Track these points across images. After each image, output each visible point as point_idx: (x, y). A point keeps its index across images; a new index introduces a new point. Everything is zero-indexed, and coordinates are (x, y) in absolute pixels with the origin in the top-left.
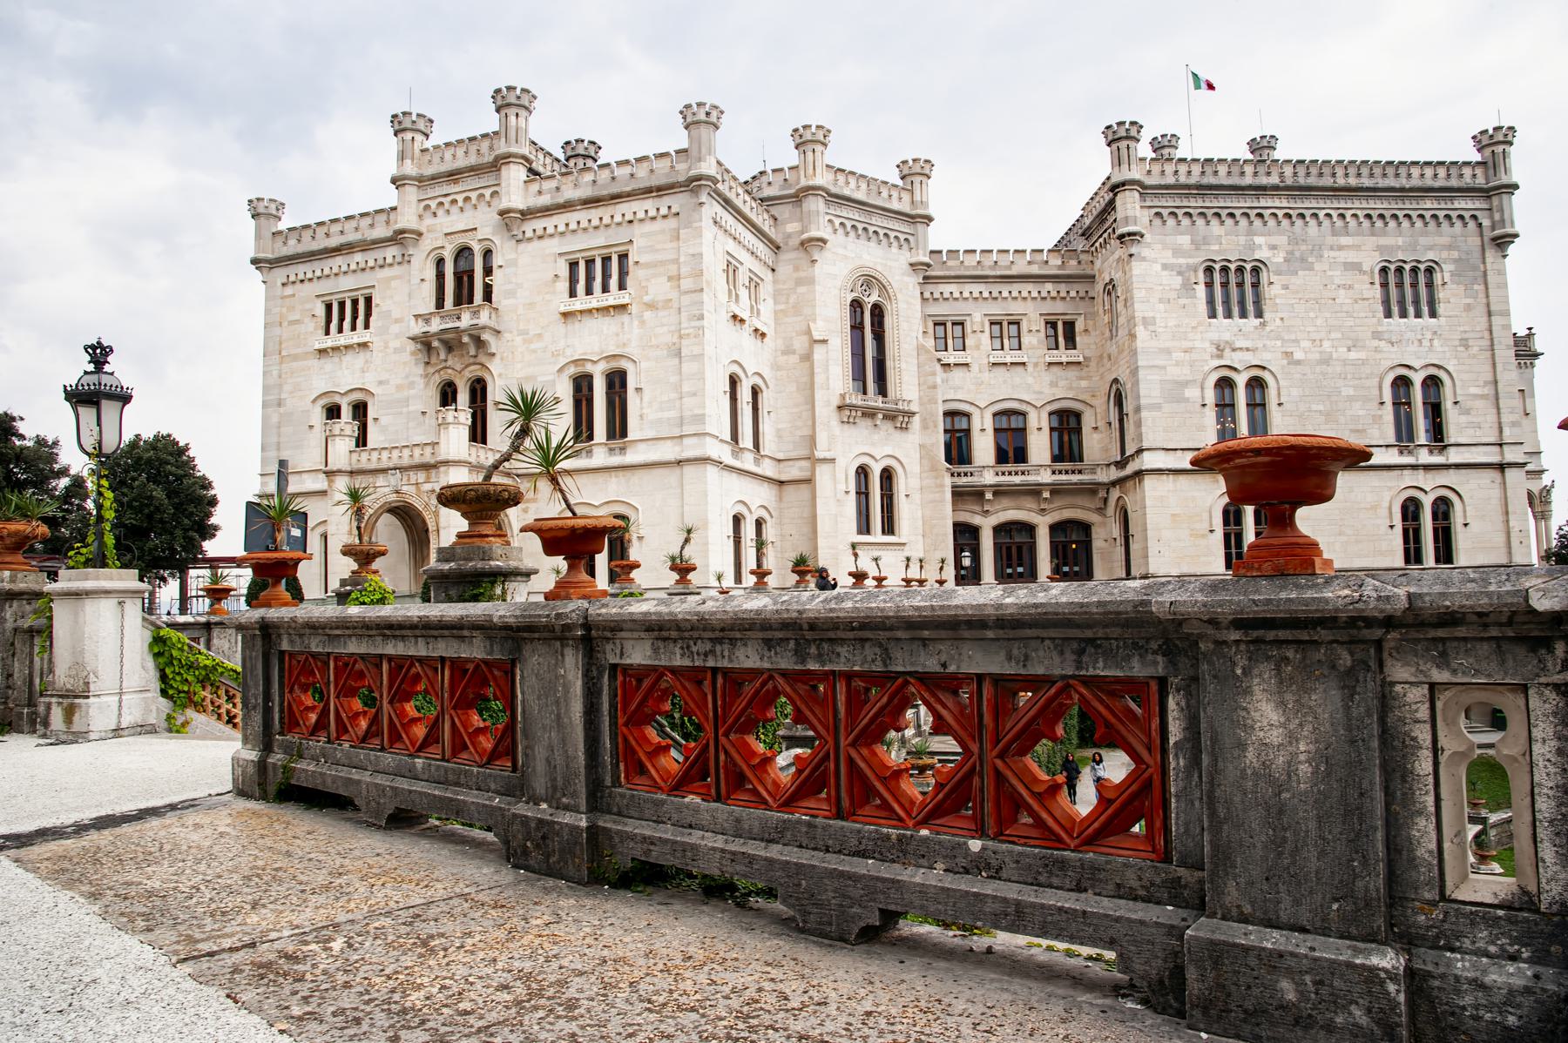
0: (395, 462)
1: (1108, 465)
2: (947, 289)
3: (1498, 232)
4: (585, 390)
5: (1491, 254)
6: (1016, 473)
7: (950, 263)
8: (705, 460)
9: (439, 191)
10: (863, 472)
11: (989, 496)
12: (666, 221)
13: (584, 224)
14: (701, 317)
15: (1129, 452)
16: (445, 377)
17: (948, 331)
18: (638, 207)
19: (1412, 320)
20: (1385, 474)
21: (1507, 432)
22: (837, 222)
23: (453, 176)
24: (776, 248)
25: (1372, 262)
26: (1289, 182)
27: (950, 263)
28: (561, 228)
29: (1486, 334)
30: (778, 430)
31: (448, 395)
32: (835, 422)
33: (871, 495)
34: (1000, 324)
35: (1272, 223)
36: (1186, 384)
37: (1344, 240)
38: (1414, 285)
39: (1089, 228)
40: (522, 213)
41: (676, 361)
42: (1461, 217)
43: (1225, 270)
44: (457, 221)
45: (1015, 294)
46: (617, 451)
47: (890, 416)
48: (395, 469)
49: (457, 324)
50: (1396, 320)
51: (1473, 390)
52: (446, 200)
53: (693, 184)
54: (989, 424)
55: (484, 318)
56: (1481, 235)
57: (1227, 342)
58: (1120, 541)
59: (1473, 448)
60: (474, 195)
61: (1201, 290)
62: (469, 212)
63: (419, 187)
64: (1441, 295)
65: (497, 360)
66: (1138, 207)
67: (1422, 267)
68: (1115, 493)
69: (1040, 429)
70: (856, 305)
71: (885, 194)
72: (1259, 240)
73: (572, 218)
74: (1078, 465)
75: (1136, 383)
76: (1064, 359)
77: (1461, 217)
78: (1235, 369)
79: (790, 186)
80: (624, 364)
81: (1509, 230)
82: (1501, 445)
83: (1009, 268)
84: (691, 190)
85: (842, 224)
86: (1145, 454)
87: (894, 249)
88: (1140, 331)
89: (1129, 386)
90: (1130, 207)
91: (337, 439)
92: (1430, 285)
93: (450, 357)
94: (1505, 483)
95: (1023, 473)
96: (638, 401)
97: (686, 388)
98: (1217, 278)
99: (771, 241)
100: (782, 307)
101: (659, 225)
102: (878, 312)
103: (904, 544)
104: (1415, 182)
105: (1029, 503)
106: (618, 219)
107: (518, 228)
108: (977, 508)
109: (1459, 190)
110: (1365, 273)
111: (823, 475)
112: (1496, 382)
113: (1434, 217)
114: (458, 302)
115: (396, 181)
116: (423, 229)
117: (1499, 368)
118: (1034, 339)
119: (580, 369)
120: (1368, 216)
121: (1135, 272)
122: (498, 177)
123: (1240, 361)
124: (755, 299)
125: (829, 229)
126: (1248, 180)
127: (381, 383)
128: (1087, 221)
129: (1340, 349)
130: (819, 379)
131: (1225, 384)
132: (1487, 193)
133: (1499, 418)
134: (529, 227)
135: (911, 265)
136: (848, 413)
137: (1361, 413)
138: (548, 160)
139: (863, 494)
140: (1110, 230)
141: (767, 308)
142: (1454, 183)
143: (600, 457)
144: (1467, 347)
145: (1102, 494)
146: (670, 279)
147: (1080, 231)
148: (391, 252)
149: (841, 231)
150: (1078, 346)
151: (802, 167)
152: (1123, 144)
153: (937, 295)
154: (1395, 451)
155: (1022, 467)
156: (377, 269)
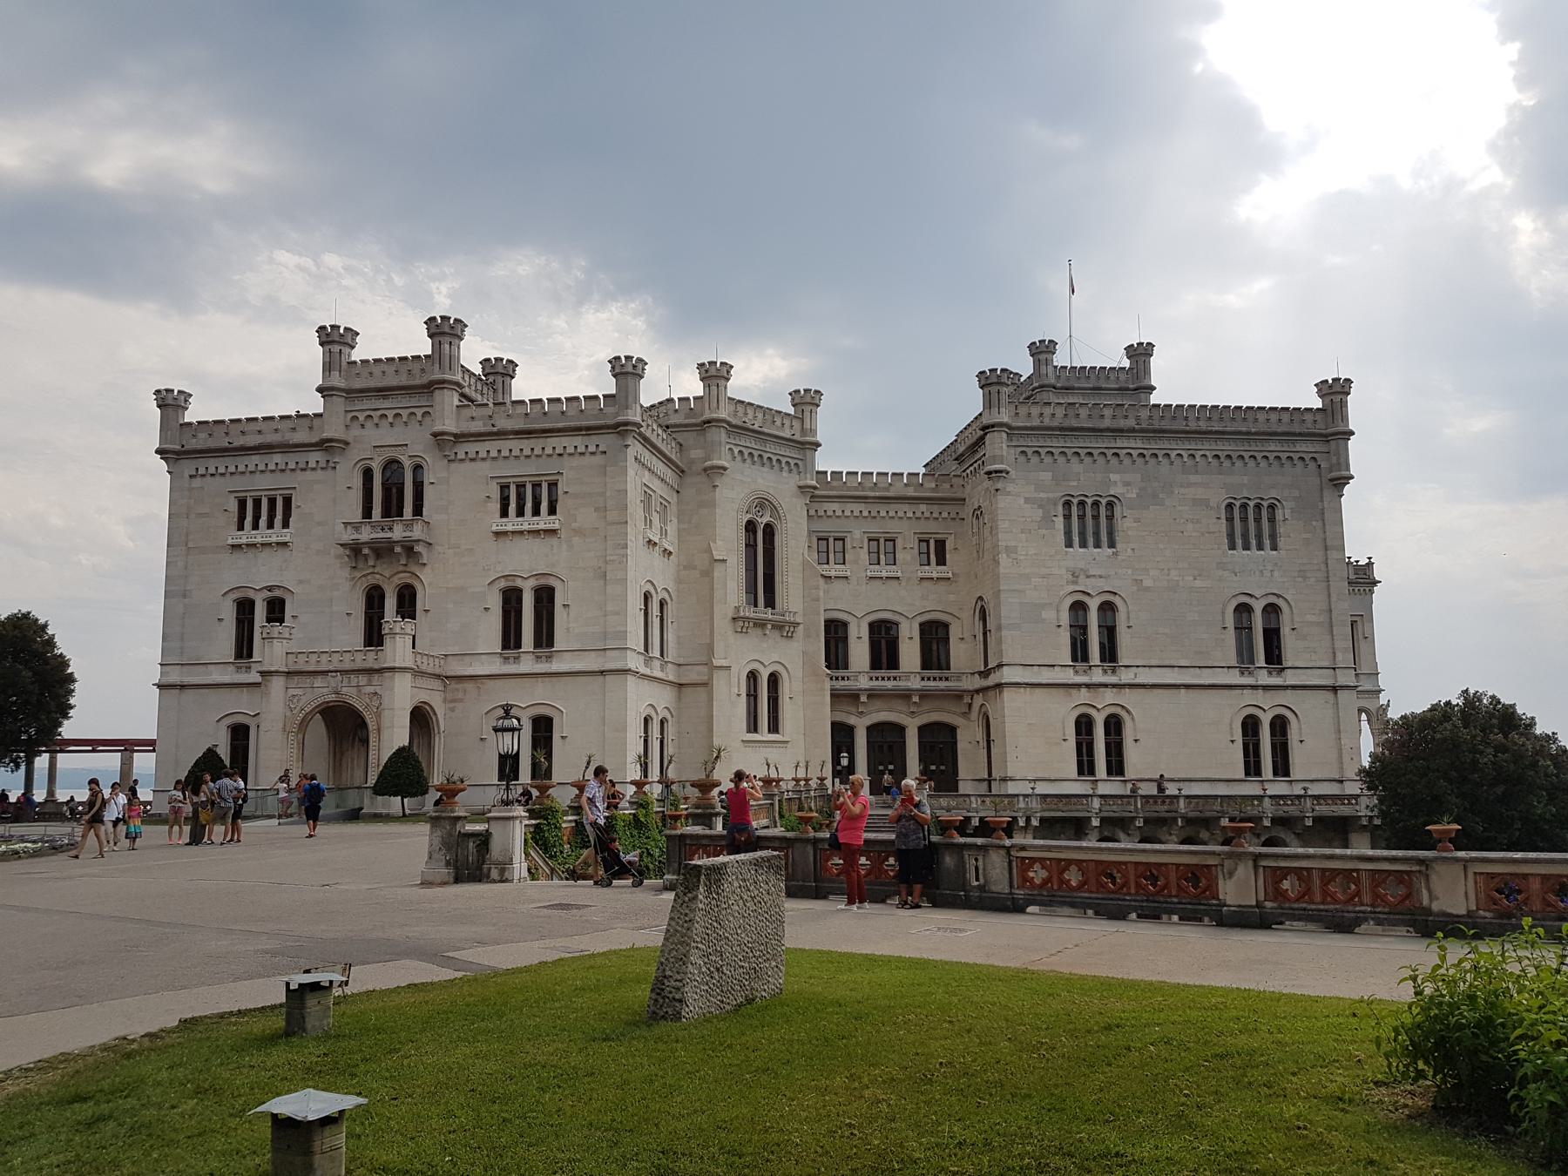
0: (335, 665)
1: (973, 674)
3: (1335, 474)
4: (514, 603)
5: (1328, 494)
6: (889, 679)
7: (835, 484)
8: (626, 671)
9: (367, 404)
10: (753, 676)
11: (863, 699)
12: (593, 457)
13: (516, 452)
14: (626, 546)
16: (372, 580)
17: (829, 546)
18: (570, 442)
19: (1254, 553)
20: (1226, 692)
21: (1340, 656)
23: (383, 392)
24: (681, 472)
25: (1219, 498)
26: (1144, 426)
27: (835, 484)
28: (494, 454)
29: (1323, 567)
30: (679, 637)
31: (374, 599)
32: (730, 633)
33: (759, 700)
34: (878, 540)
35: (1127, 461)
36: (1043, 606)
37: (1193, 478)
38: (1258, 520)
39: (962, 455)
40: (455, 435)
41: (602, 582)
42: (1302, 459)
43: (1082, 504)
44: (387, 436)
45: (892, 514)
46: (544, 659)
47: (778, 627)
48: (336, 671)
49: (389, 535)
50: (1240, 552)
51: (1310, 618)
52: (376, 414)
53: (621, 429)
54: (865, 632)
55: (417, 532)
56: (1320, 477)
57: (1082, 569)
58: (983, 744)
59: (1309, 670)
60: (405, 413)
61: (1060, 522)
62: (399, 428)
63: (346, 398)
64: (1282, 530)
65: (427, 570)
66: (1004, 446)
67: (1265, 504)
68: (978, 700)
70: (751, 527)
71: (778, 423)
72: (1113, 477)
73: (505, 445)
74: (945, 673)
75: (998, 604)
76: (935, 575)
77: (1302, 459)
78: (1089, 594)
79: (694, 416)
80: (552, 582)
81: (1344, 473)
82: (1334, 669)
83: (887, 489)
84: (617, 433)
85: (740, 452)
86: (1005, 668)
88: (1003, 558)
89: (991, 605)
90: (997, 445)
91: (275, 641)
92: (1272, 520)
93: (378, 562)
94: (1337, 704)
95: (895, 679)
96: (565, 616)
97: (609, 608)
98: (1074, 509)
99: (677, 467)
100: (686, 526)
101: (587, 459)
102: (769, 531)
104: (1262, 427)
105: (900, 705)
106: (549, 451)
107: (450, 450)
108: (853, 710)
109: (1300, 434)
110: (1212, 508)
111: (719, 682)
112: (1331, 611)
113: (1278, 458)
114: (386, 513)
115: (320, 390)
116: (350, 439)
117: (1334, 599)
118: (907, 554)
119: (510, 584)
120: (1217, 456)
121: (1001, 505)
122: (432, 400)
123: (1093, 587)
124: (664, 521)
125: (729, 457)
126: (1107, 423)
127: (301, 582)
128: (961, 449)
129: (1186, 578)
130: (718, 594)
131: (1078, 608)
132: (1326, 438)
133: (1333, 644)
134: (461, 450)
135: (799, 487)
136: (741, 624)
137: (1205, 636)
138: (473, 381)
139: (752, 696)
140: (980, 462)
141: (672, 529)
142: (1297, 428)
143: (527, 665)
144: (1305, 578)
145: (967, 699)
146: (597, 510)
147: (954, 456)
148: (314, 457)
149: (739, 458)
150: (947, 564)
151: (707, 398)
152: (994, 389)
153: (821, 513)
154: (1237, 671)
155: (893, 673)
156: (298, 472)
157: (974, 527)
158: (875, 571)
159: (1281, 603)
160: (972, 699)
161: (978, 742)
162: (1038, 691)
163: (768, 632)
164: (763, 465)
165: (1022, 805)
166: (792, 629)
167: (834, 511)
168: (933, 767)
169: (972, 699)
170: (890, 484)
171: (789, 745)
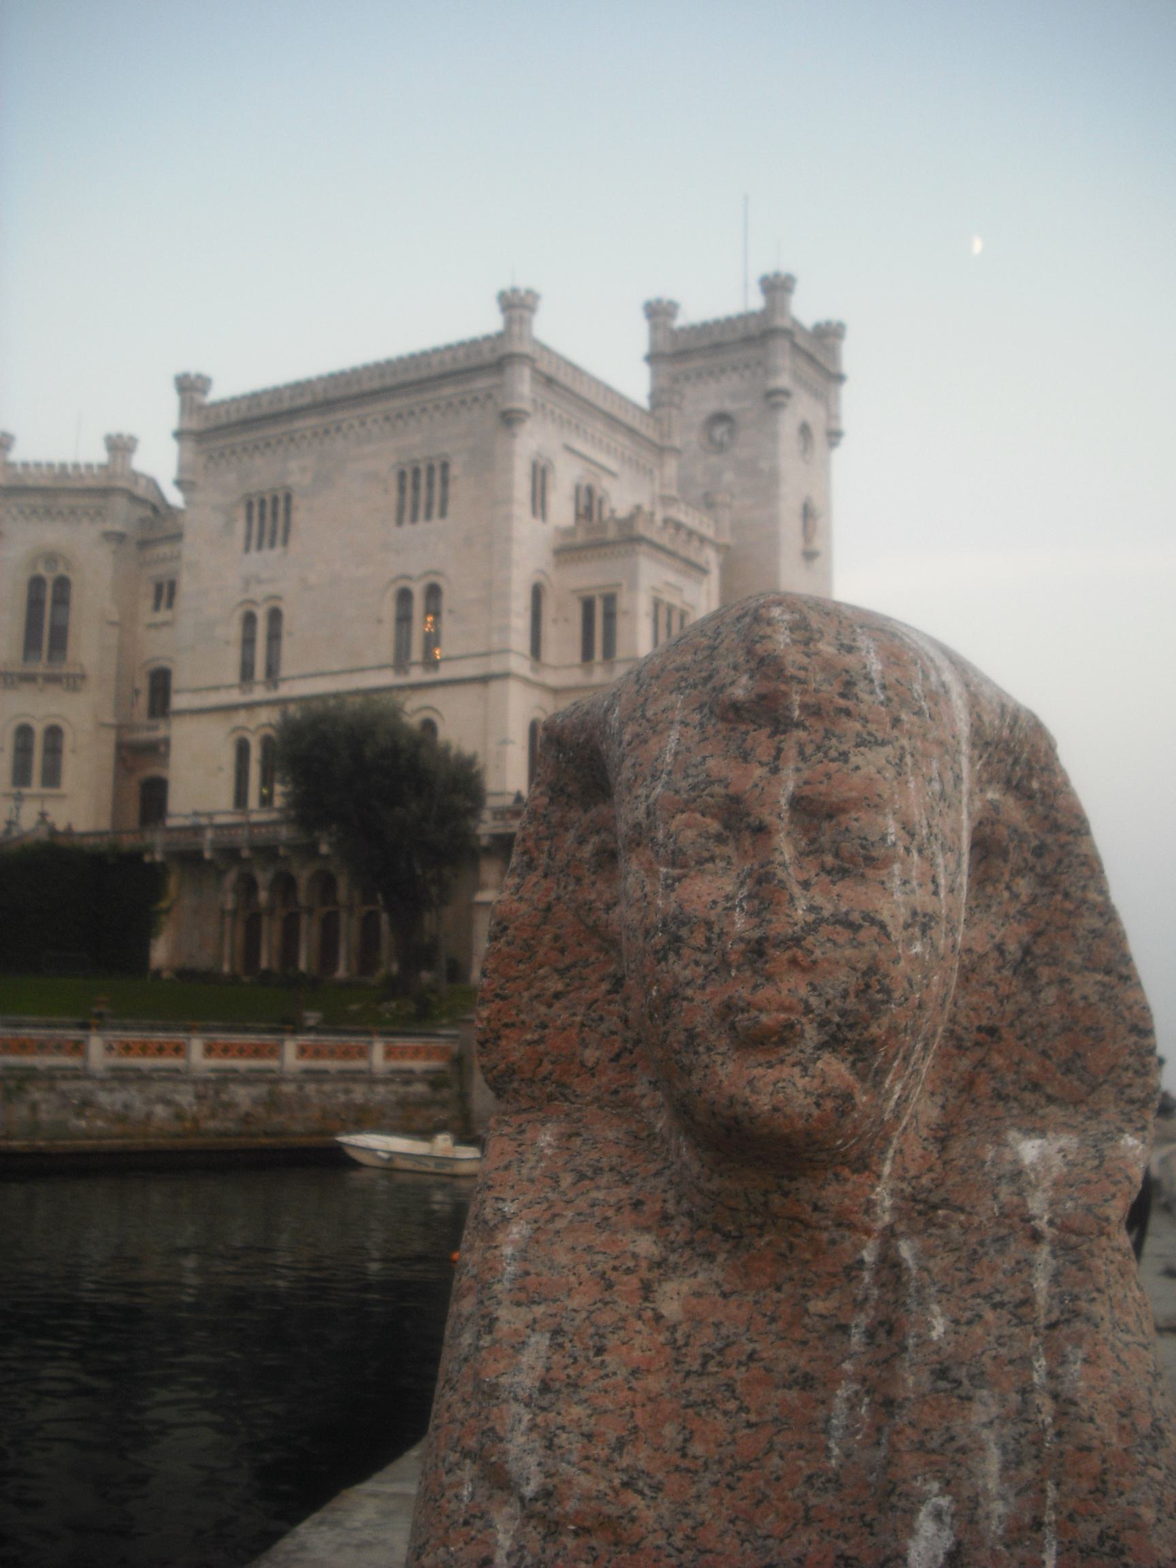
10: (24, 733)
61: (240, 527)
70: (36, 584)
72: (293, 465)
92: (445, 482)
102: (63, 584)
120: (387, 419)
131: (249, 620)
159: (441, 582)
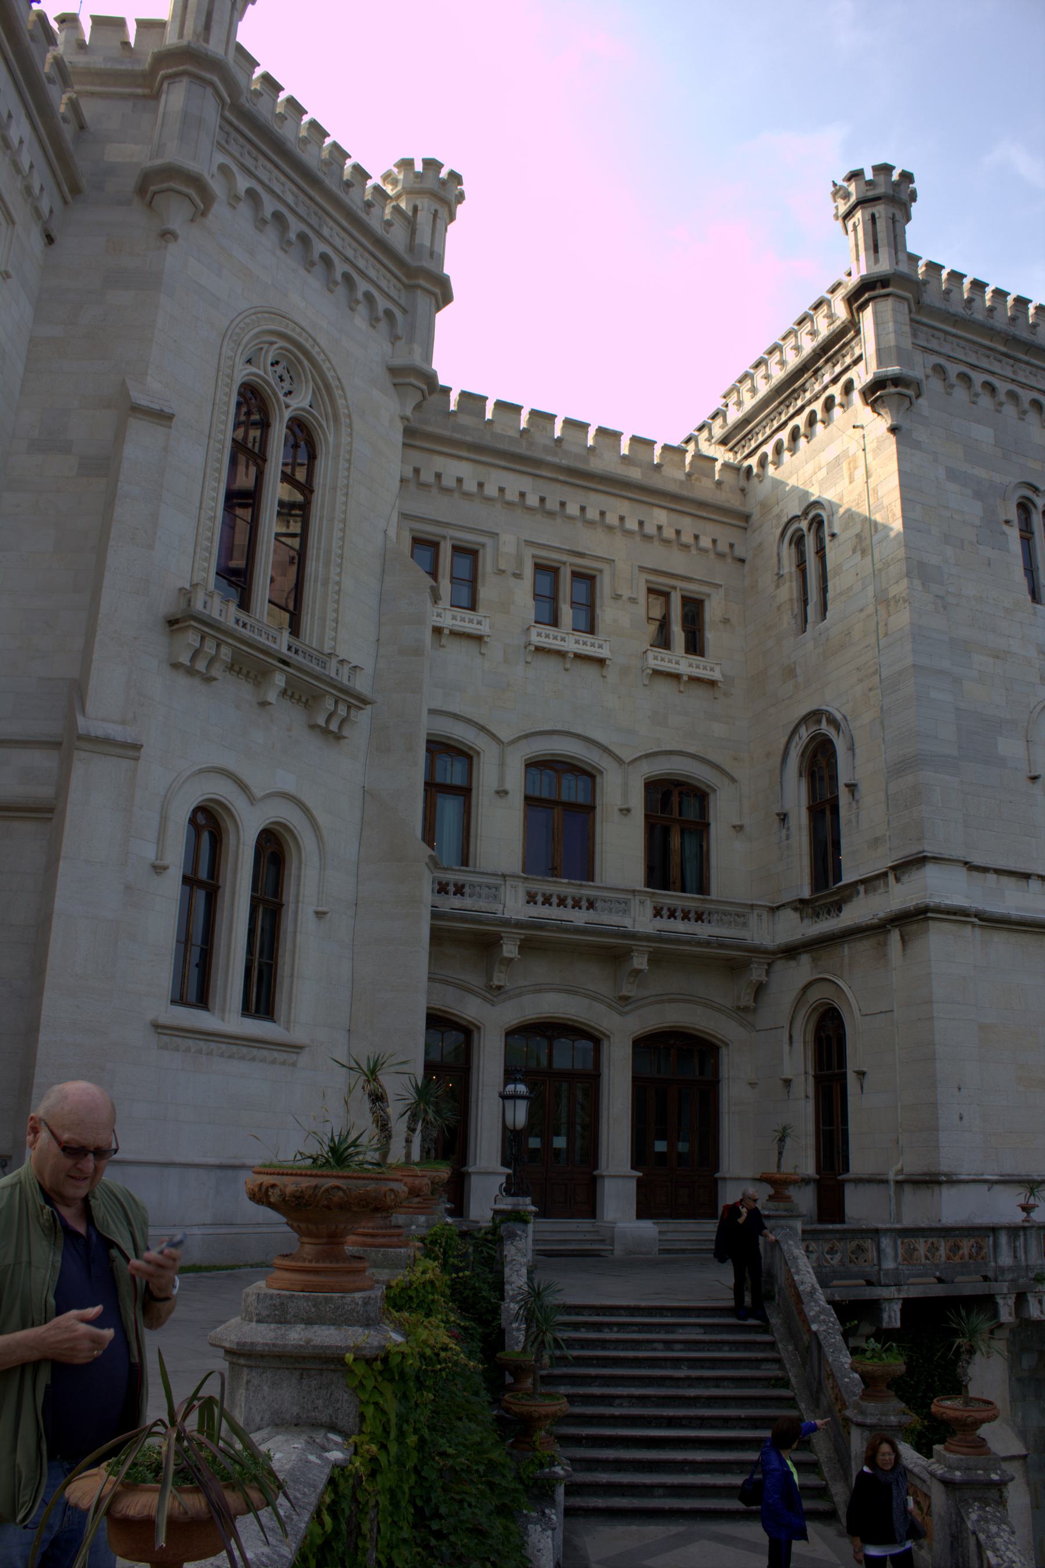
1: (774, 910)
2: (454, 469)
6: (577, 904)
7: (465, 420)
11: (510, 949)
15: (847, 878)
22: (243, 183)
54: (515, 780)
58: (805, 1087)
69: (626, 811)
87: (360, 320)
95: (591, 905)
103: (297, 1048)
108: (475, 980)
135: (393, 371)
145: (757, 974)
153: (427, 477)
157: (785, 561)
158: (543, 636)
160: (768, 972)
161: (787, 1082)
162: (1001, 942)
163: (272, 696)
164: (309, 265)
165: (1005, 1259)
166: (342, 710)
167: (460, 481)
168: (660, 1146)
169: (768, 972)
170: (592, 449)
171: (303, 1059)
